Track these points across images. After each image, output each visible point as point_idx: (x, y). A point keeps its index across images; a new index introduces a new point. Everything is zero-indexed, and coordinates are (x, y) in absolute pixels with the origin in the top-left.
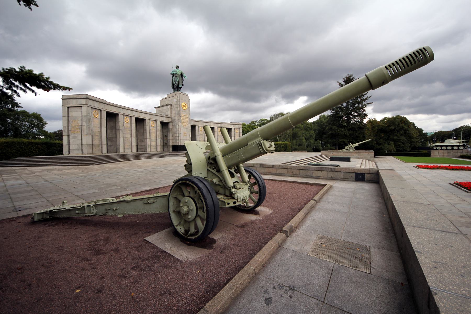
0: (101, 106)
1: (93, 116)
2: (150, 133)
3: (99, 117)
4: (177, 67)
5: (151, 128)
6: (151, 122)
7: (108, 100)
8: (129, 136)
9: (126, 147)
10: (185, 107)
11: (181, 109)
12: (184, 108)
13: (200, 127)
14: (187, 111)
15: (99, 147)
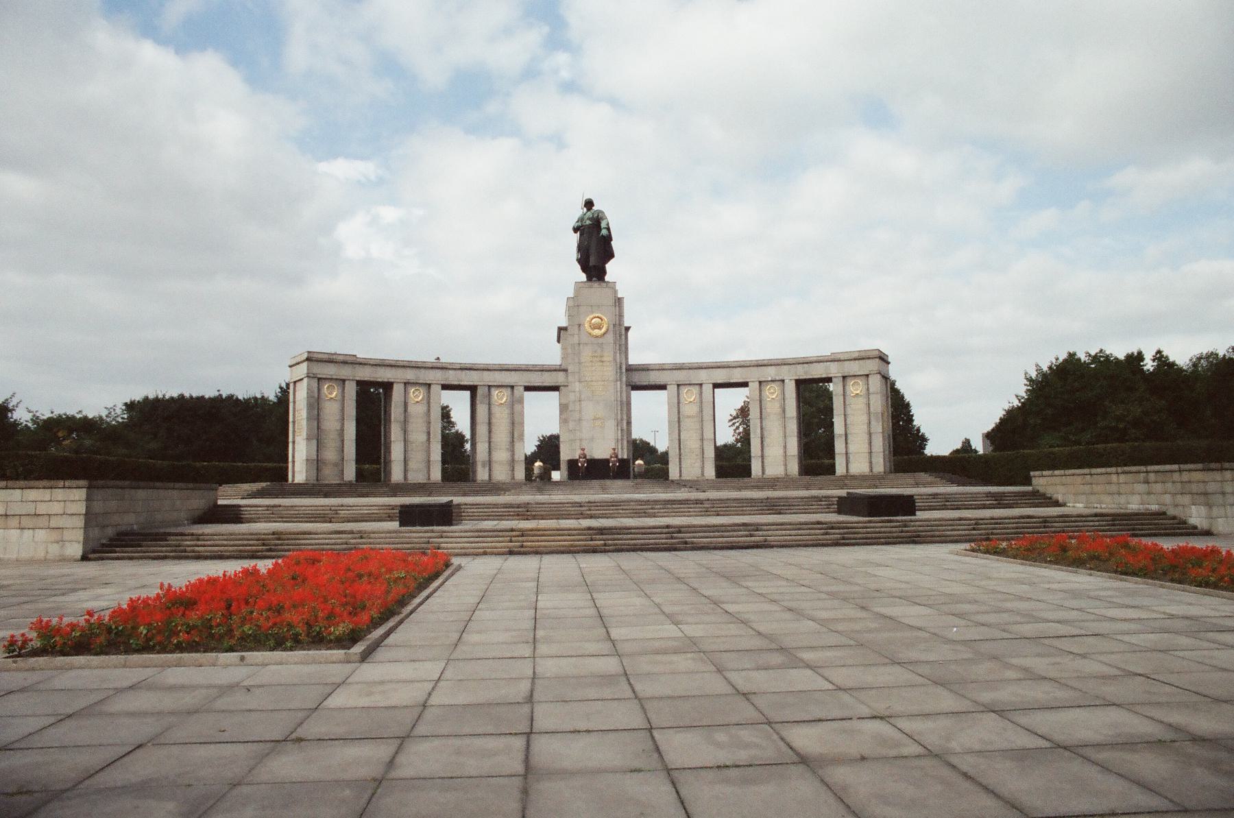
0: (345, 372)
1: (323, 396)
2: (490, 424)
3: (339, 397)
4: (589, 204)
5: (495, 410)
6: (495, 392)
7: (361, 355)
8: (424, 437)
9: (411, 465)
10: (600, 328)
11: (585, 339)
12: (597, 332)
13: (684, 390)
14: (610, 338)
15: (336, 465)
